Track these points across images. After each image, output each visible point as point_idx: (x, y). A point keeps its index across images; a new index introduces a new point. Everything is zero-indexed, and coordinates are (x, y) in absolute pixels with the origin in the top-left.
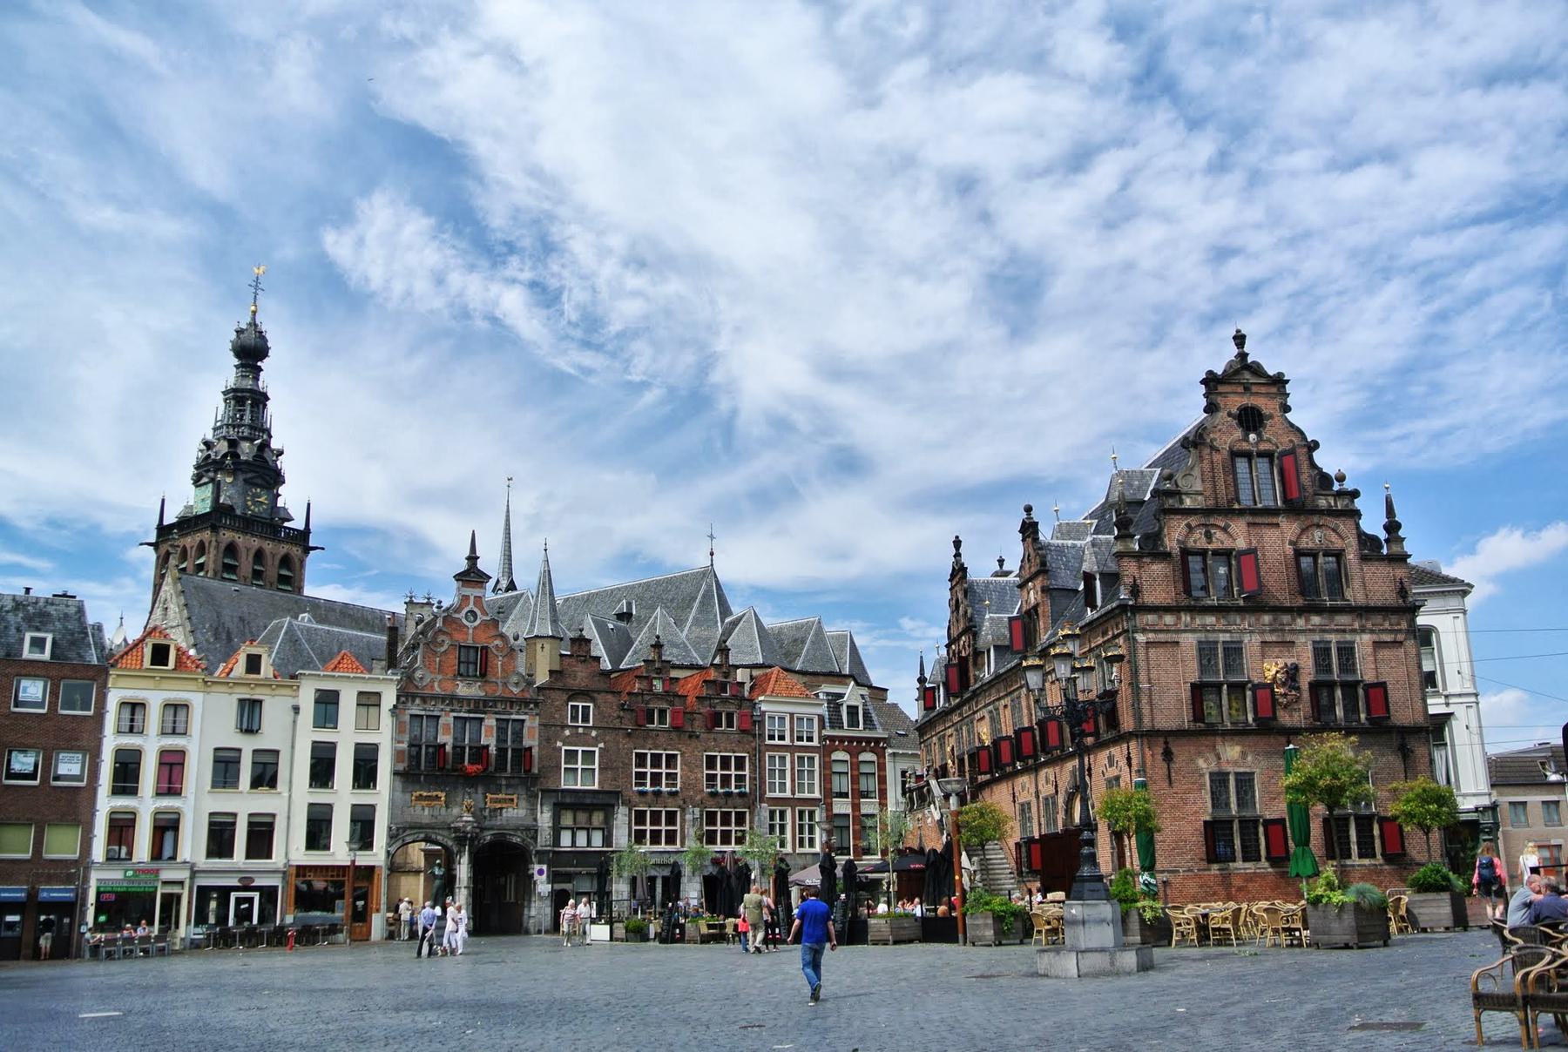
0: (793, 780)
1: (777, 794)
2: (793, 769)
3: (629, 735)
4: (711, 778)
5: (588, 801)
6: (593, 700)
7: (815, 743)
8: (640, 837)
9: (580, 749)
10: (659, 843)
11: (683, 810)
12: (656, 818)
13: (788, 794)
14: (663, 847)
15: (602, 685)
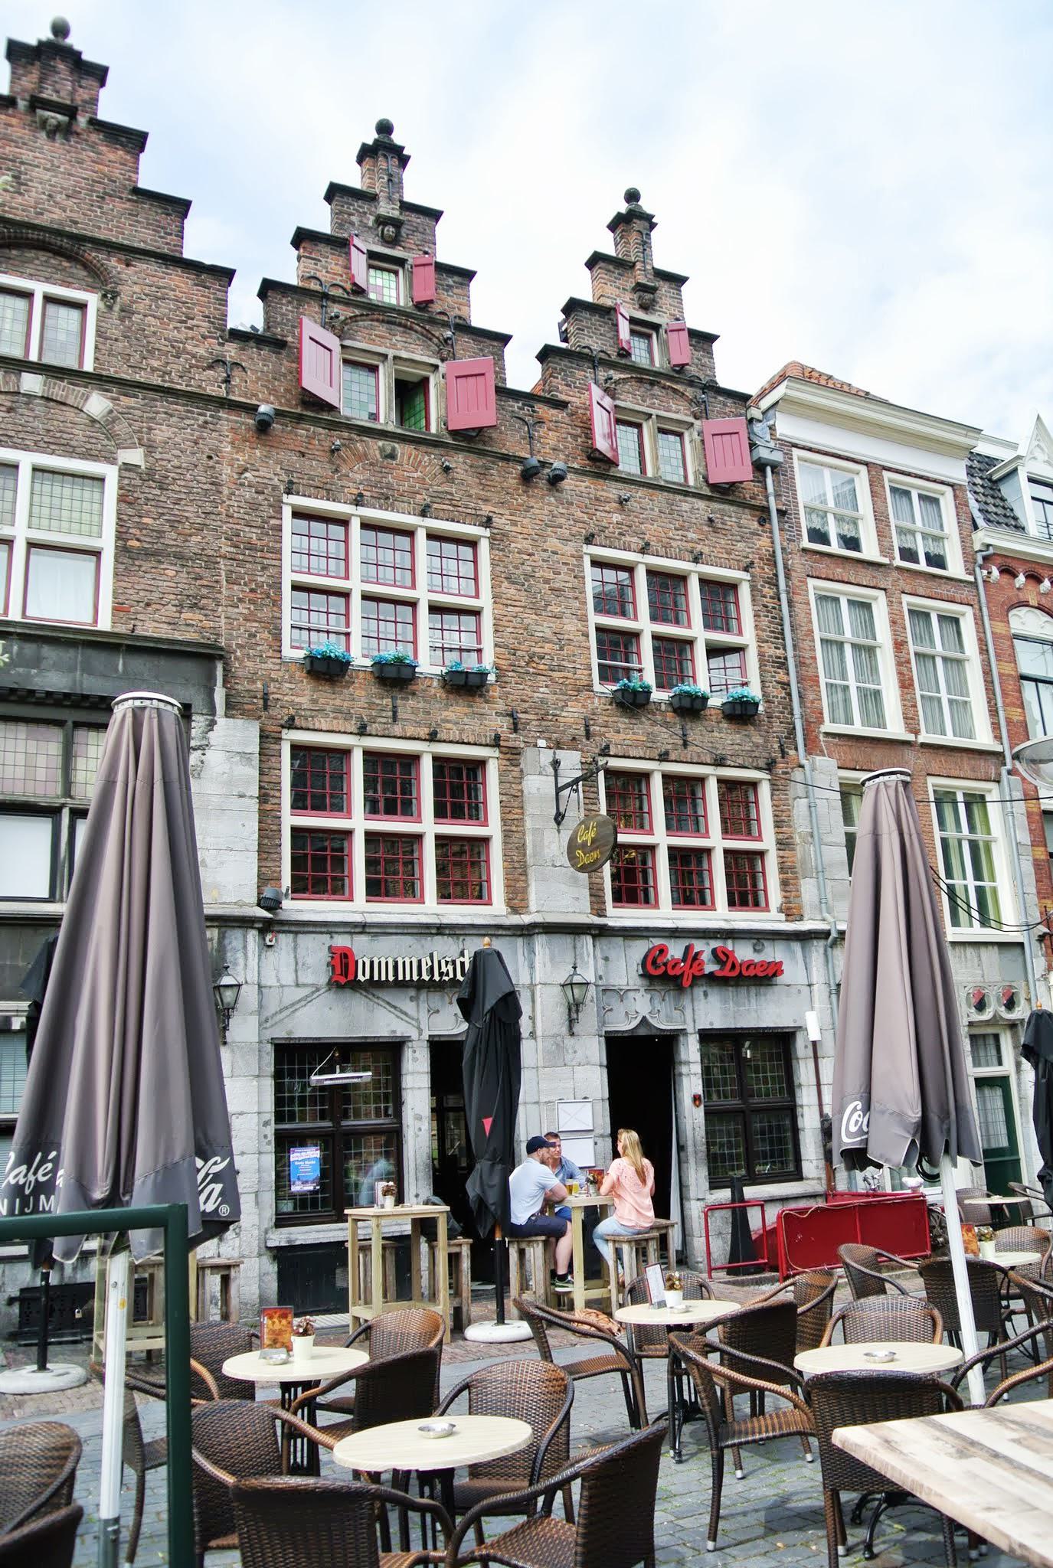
0: (906, 684)
1: (858, 728)
2: (899, 645)
3: (263, 427)
4: (617, 644)
5: (53, 679)
6: (97, 278)
7: (956, 568)
8: (318, 864)
9: (26, 460)
10: (410, 891)
11: (512, 755)
12: (390, 781)
13: (895, 728)
14: (430, 908)
15: (142, 236)
